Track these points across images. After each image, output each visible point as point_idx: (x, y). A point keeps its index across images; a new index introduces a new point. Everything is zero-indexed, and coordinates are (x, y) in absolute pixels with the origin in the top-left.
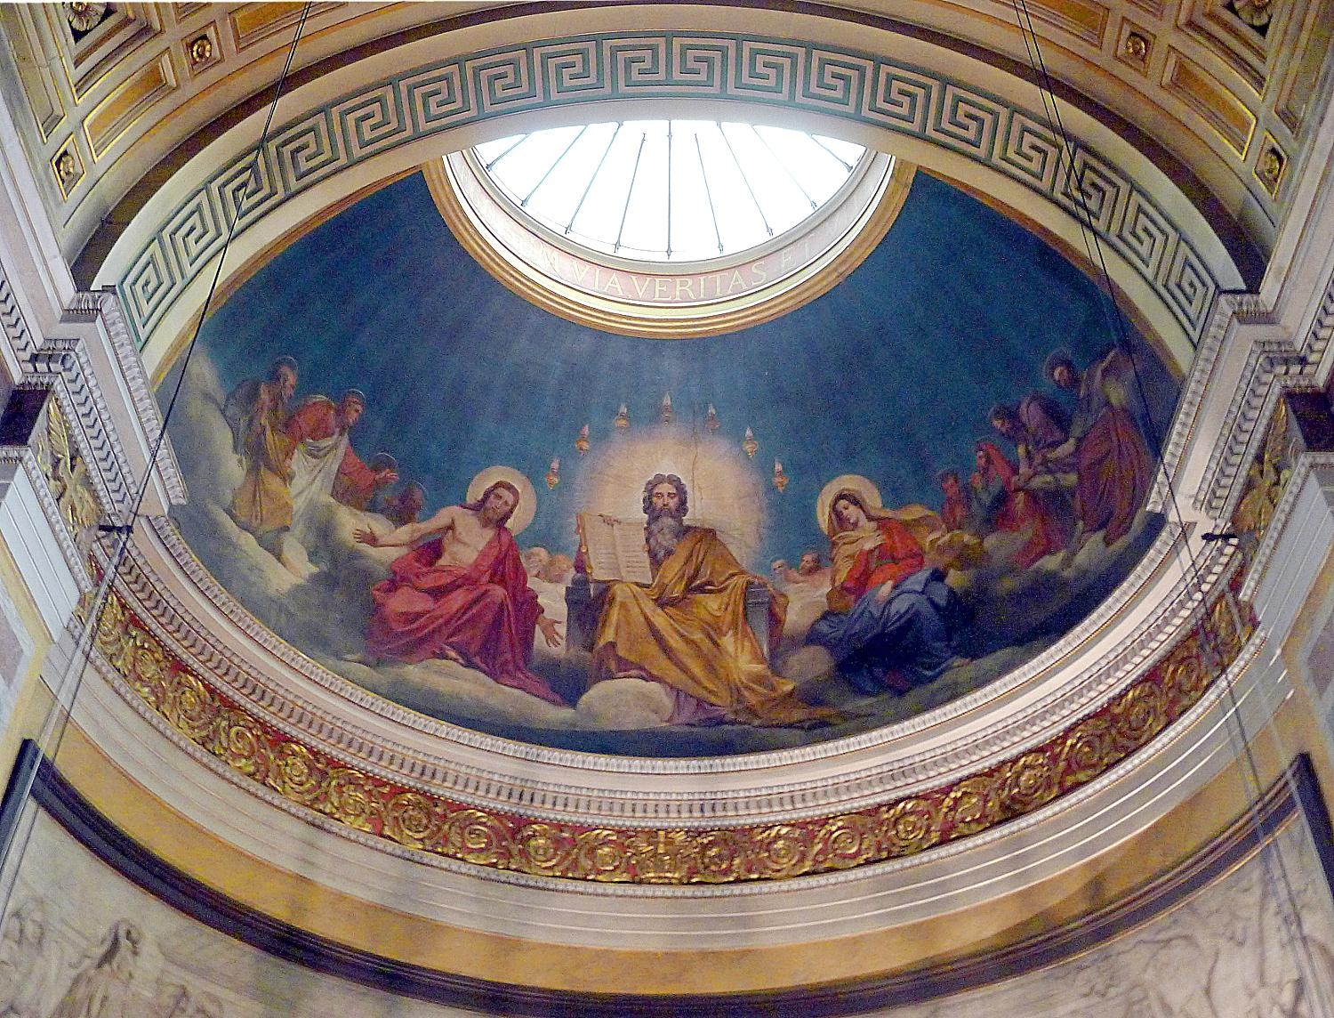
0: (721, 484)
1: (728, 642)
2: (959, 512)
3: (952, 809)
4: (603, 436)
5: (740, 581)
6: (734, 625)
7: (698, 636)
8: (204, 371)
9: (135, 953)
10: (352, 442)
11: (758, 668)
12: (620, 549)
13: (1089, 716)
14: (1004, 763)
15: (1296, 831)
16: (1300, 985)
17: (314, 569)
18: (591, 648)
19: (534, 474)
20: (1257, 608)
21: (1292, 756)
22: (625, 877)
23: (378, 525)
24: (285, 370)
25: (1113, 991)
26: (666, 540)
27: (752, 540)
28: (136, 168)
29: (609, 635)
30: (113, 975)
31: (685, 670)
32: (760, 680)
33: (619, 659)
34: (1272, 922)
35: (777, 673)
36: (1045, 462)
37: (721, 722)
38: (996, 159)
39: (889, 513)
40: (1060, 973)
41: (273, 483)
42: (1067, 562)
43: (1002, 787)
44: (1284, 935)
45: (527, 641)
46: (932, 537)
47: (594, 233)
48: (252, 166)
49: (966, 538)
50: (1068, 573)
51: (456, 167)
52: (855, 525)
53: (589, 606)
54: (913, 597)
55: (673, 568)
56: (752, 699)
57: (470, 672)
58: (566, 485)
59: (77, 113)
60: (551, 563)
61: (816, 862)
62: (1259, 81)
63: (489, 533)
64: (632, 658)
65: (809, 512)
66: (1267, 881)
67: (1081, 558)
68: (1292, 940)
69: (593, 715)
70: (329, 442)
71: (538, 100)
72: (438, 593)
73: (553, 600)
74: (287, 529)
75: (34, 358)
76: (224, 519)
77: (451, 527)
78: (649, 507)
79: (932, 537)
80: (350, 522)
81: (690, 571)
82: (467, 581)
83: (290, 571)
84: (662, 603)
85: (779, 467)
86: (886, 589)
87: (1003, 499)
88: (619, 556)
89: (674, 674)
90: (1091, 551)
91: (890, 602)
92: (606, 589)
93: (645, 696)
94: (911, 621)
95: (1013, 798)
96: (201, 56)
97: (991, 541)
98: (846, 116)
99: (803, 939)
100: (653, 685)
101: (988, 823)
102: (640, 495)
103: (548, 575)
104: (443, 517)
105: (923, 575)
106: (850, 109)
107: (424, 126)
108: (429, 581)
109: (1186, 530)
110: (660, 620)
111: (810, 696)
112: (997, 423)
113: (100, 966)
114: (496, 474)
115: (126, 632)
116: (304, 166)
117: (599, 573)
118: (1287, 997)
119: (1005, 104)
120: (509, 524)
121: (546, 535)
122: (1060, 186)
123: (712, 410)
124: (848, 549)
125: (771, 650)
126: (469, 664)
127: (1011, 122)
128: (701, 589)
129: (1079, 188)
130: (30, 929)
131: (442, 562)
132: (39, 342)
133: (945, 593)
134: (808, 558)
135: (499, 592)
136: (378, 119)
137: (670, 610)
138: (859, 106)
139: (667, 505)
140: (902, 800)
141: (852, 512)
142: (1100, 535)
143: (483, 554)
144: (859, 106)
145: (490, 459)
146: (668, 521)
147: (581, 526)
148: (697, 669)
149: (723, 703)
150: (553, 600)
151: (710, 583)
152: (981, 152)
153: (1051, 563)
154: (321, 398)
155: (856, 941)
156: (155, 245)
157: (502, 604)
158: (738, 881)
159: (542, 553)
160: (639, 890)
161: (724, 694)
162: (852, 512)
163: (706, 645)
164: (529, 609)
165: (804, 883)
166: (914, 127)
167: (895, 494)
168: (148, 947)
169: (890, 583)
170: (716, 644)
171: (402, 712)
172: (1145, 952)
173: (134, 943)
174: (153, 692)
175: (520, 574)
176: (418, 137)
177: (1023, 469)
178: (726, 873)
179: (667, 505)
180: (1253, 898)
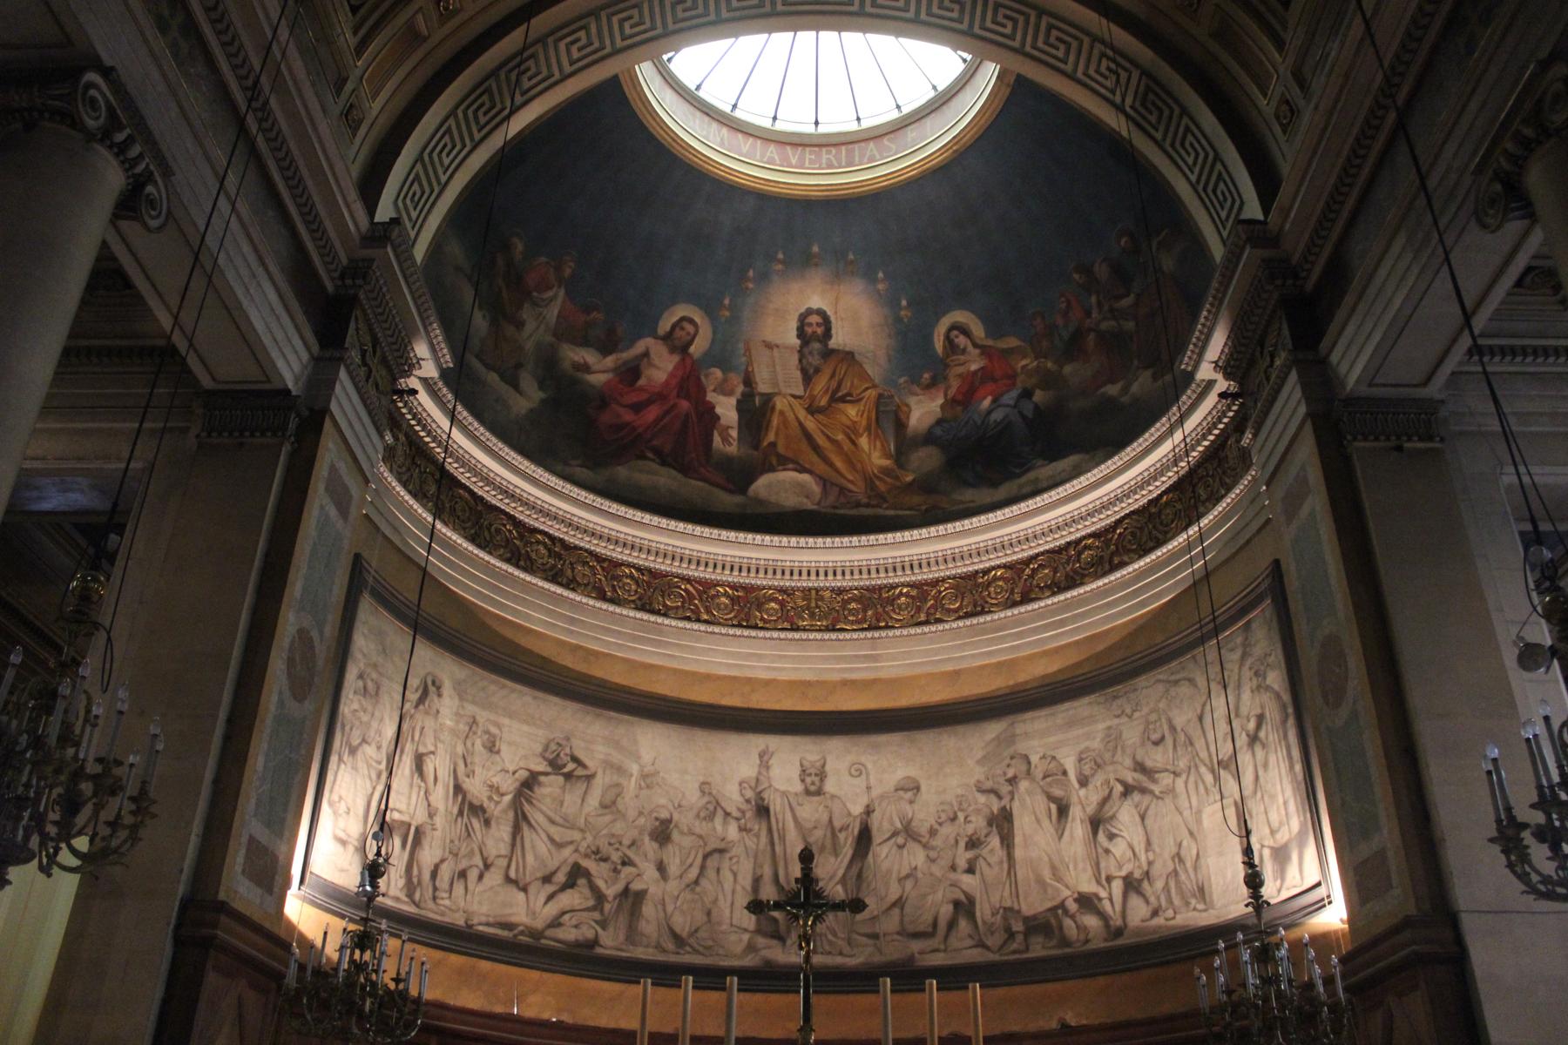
0: (855, 315)
1: (864, 441)
2: (1045, 344)
3: (1032, 576)
4: (764, 278)
5: (872, 393)
6: (868, 428)
7: (840, 437)
8: (456, 251)
9: (440, 695)
10: (567, 293)
11: (886, 462)
12: (778, 368)
13: (1132, 513)
14: (1069, 544)
15: (1267, 614)
16: (1260, 719)
17: (541, 395)
18: (756, 447)
19: (710, 310)
20: (1253, 452)
21: (1271, 559)
22: (786, 625)
23: (589, 356)
24: (515, 240)
25: (1137, 715)
26: (815, 360)
27: (883, 360)
28: (400, 102)
29: (771, 437)
30: (427, 713)
31: (831, 465)
32: (886, 471)
33: (779, 456)
34: (1247, 673)
36: (1112, 310)
37: (858, 505)
38: (1079, 74)
39: (990, 342)
40: (1102, 699)
41: (510, 330)
42: (1125, 390)
43: (1068, 562)
44: (1255, 681)
45: (709, 441)
46: (1024, 362)
47: (755, 112)
48: (488, 91)
49: (1049, 365)
50: (1125, 399)
51: (645, 72)
52: (964, 351)
53: (755, 413)
54: (1008, 410)
55: (821, 384)
56: (882, 487)
57: (664, 470)
59: (358, 72)
60: (725, 380)
61: (928, 614)
62: (1280, 45)
63: (676, 358)
64: (790, 455)
65: (928, 339)
66: (1246, 645)
67: (1135, 388)
68: (1259, 687)
69: (760, 502)
70: (550, 294)
71: (712, 17)
72: (637, 408)
73: (727, 410)
74: (519, 366)
75: (342, 277)
76: (476, 364)
77: (646, 354)
78: (801, 333)
79: (1024, 362)
81: (834, 384)
82: (659, 396)
83: (527, 399)
84: (812, 410)
85: (904, 303)
86: (987, 403)
87: (1077, 337)
88: (778, 374)
89: (821, 467)
90: (1142, 383)
91: (989, 412)
92: (768, 398)
94: (1005, 427)
95: (1074, 571)
96: (446, 9)
97: (1067, 369)
98: (962, 33)
99: (918, 671)
100: (806, 477)
101: (1057, 588)
102: (793, 325)
104: (640, 347)
105: (1014, 393)
106: (964, 26)
107: (619, 43)
108: (633, 398)
109: (1210, 384)
110: (810, 424)
111: (925, 485)
112: (1076, 276)
113: (416, 707)
114: (681, 311)
115: (414, 463)
116: (526, 84)
117: (763, 387)
118: (1252, 725)
119: (1088, 33)
120: (692, 349)
121: (721, 357)
122: (1129, 101)
123: (851, 257)
124: (960, 370)
125: (897, 449)
126: (663, 463)
127: (1092, 48)
128: (843, 400)
129: (1143, 105)
130: (370, 684)
131: (642, 382)
132: (345, 261)
133: (1031, 406)
134: (926, 376)
135: (685, 405)
136: (584, 41)
137: (820, 417)
138: (971, 25)
139: (814, 333)
140: (993, 568)
141: (961, 340)
142: (1148, 373)
143: (672, 375)
144: (971, 25)
145: (674, 301)
146: (816, 346)
147: (748, 350)
148: (839, 464)
149: (858, 489)
150: (727, 410)
151: (849, 394)
152: (1069, 68)
153: (1112, 390)
154: (543, 259)
155: (957, 673)
156: (419, 167)
157: (687, 415)
158: (870, 628)
159: (718, 373)
160: (797, 635)
161: (861, 484)
162: (961, 340)
163: (847, 446)
164: (708, 417)
165: (919, 630)
166: (1016, 44)
167: (994, 329)
168: (447, 689)
169: (989, 399)
170: (853, 443)
171: (615, 508)
172: (1161, 687)
173: (439, 688)
174: (436, 505)
175: (702, 390)
176: (616, 52)
177: (1095, 315)
178: (864, 620)
179: (814, 333)
180: (1236, 655)
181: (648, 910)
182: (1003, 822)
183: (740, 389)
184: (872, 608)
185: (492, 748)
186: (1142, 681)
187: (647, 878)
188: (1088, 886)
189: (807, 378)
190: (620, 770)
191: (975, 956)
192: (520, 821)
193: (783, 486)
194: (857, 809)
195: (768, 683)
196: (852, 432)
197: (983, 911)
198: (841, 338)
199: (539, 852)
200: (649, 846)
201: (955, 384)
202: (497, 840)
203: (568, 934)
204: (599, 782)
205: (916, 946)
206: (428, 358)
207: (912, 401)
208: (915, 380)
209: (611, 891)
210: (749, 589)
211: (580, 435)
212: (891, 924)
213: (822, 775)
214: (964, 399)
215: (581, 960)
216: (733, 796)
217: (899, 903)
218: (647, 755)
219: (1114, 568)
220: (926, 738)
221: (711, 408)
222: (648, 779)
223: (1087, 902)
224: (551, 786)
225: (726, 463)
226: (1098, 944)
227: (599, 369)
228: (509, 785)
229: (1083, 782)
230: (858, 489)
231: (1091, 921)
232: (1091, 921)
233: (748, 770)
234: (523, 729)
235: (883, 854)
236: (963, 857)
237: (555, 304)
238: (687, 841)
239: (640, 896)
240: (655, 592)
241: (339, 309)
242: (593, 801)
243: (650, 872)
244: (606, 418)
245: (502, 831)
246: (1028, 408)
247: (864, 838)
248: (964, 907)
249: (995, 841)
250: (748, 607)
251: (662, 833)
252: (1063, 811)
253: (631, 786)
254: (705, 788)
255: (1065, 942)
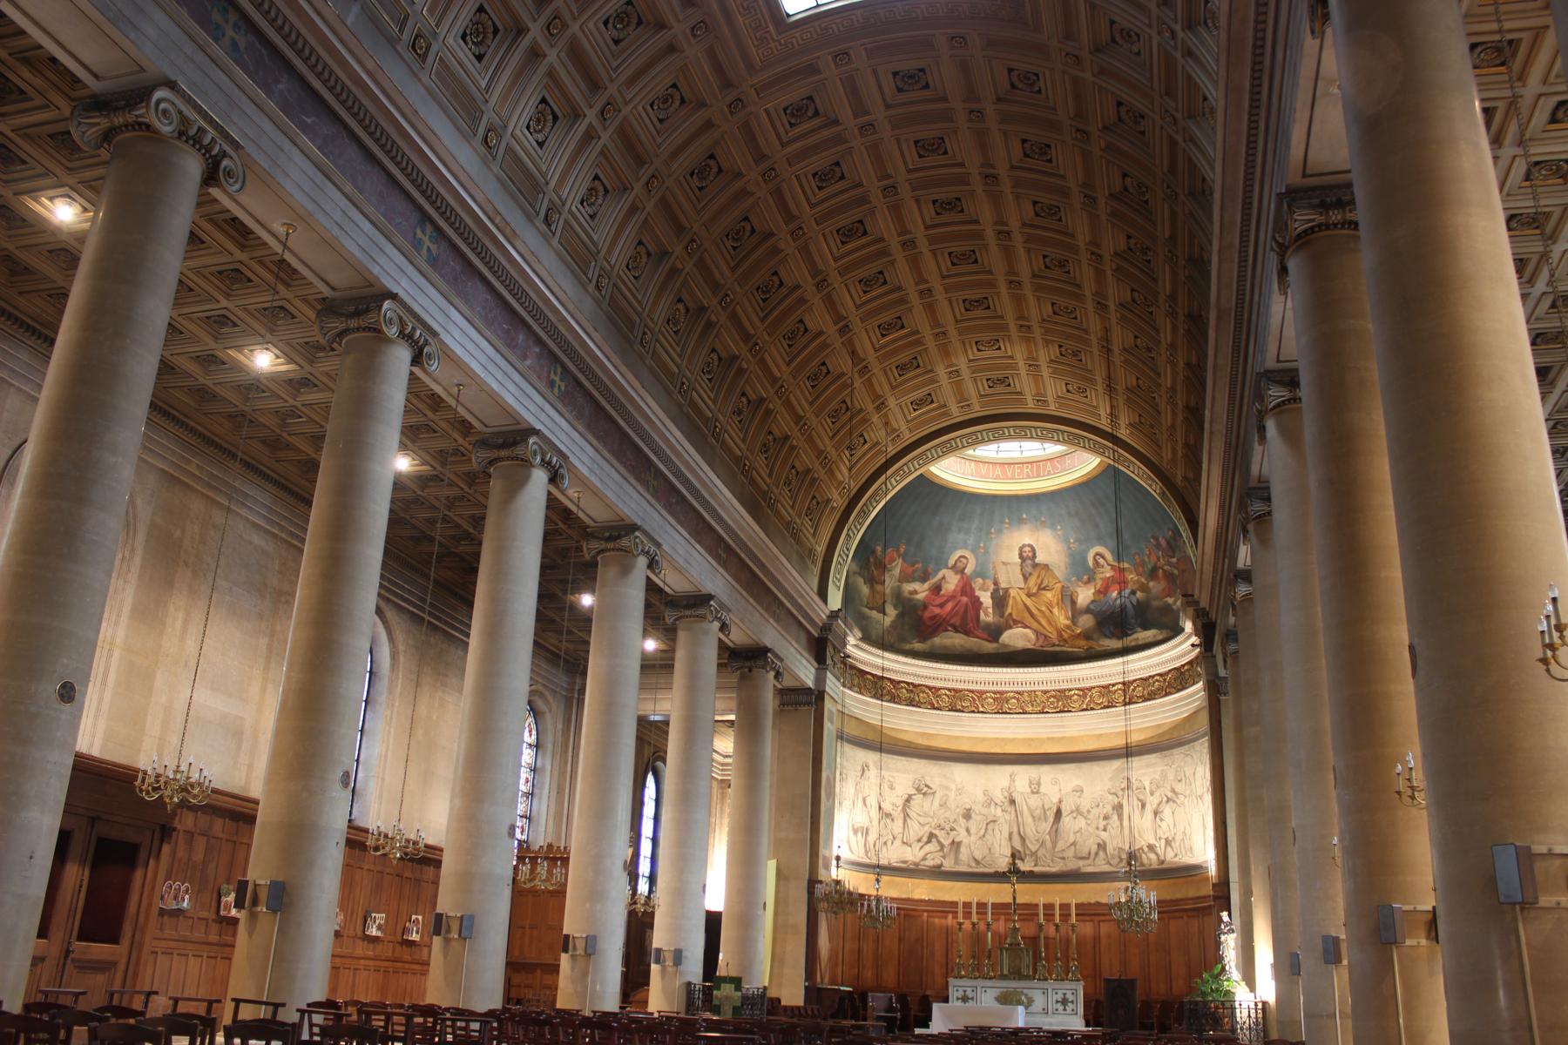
0: (1049, 545)
1: (1055, 610)
4: (999, 531)
5: (1059, 586)
23: (916, 586)
26: (1029, 569)
29: (1009, 610)
32: (1068, 627)
35: (1074, 623)
45: (978, 616)
53: (1000, 600)
55: (1033, 581)
58: (986, 552)
65: (1085, 560)
69: (1006, 646)
72: (941, 606)
73: (986, 599)
78: (1021, 556)
80: (908, 587)
82: (952, 597)
84: (1029, 595)
86: (1115, 594)
88: (1011, 578)
89: (1035, 625)
92: (1006, 590)
93: (1025, 635)
94: (1123, 608)
100: (1027, 631)
103: (983, 589)
104: (940, 575)
110: (1028, 602)
111: (1086, 636)
117: (1003, 585)
126: (957, 631)
135: (965, 599)
139: (1028, 557)
141: (1101, 561)
149: (1054, 636)
150: (986, 599)
162: (1101, 561)
164: (977, 603)
167: (1119, 558)
175: (972, 590)
179: (1028, 557)
181: (963, 849)
182: (1118, 808)
183: (992, 587)
184: (1061, 702)
185: (892, 788)
186: (1175, 751)
187: (961, 835)
188: (1152, 841)
189: (1026, 579)
190: (947, 788)
191: (1107, 868)
192: (906, 816)
193: (1018, 637)
194: (1055, 800)
195: (1013, 740)
196: (1050, 606)
197: (1110, 849)
198: (1041, 558)
199: (915, 830)
200: (962, 821)
201: (1099, 583)
202: (897, 826)
203: (930, 863)
204: (938, 795)
205: (1081, 863)
206: (851, 640)
207: (1079, 590)
208: (1080, 579)
209: (946, 843)
210: (1001, 693)
211: (918, 630)
212: (1070, 853)
213: (1039, 784)
214: (1103, 591)
215: (938, 873)
216: (999, 796)
217: (1074, 844)
218: (958, 780)
219: (1167, 694)
220: (1086, 766)
221: (978, 599)
222: (960, 791)
223: (1151, 848)
224: (918, 798)
225: (987, 627)
226: (1155, 866)
227: (920, 590)
228: (900, 802)
229: (1152, 794)
230: (1054, 636)
231: (1153, 856)
232: (1153, 856)
233: (1005, 783)
234: (903, 774)
235: (1066, 820)
236: (1102, 824)
237: (897, 568)
238: (979, 818)
239: (959, 843)
240: (958, 701)
241: (822, 646)
242: (936, 803)
243: (964, 833)
244: (927, 614)
245: (899, 822)
246: (1134, 601)
247: (1058, 813)
248: (1102, 846)
249: (1115, 817)
250: (1001, 704)
251: (967, 815)
252: (1143, 806)
253: (952, 795)
254: (985, 793)
255: (1142, 864)
